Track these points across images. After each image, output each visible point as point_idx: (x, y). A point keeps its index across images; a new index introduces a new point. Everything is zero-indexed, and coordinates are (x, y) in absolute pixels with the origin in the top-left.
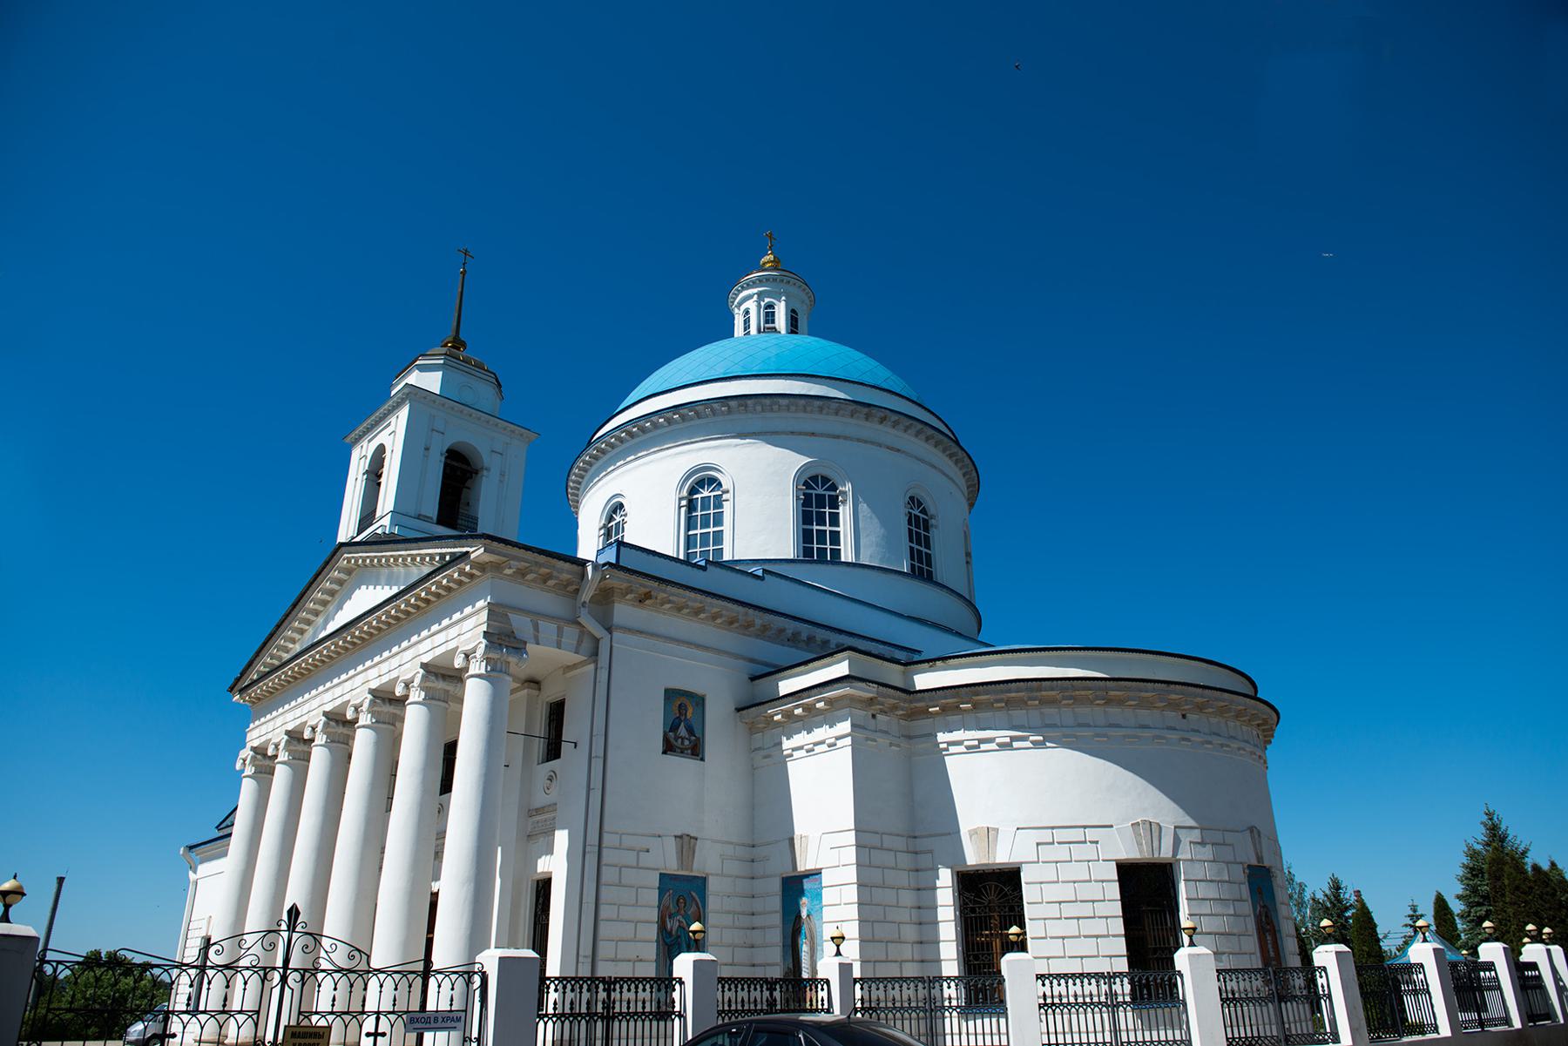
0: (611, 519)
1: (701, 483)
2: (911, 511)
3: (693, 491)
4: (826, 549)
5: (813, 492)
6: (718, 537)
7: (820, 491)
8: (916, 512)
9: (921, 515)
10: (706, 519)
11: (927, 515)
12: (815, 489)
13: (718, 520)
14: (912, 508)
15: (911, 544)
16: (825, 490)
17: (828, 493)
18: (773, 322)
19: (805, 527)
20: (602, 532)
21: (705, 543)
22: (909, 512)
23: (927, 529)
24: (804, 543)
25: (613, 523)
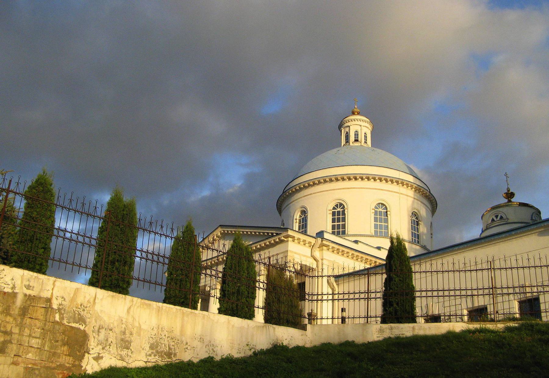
1: (337, 206)
2: (412, 218)
3: (334, 208)
5: (378, 210)
9: (416, 220)
11: (417, 219)
12: (379, 209)
13: (344, 220)
16: (382, 209)
17: (383, 211)
18: (358, 138)
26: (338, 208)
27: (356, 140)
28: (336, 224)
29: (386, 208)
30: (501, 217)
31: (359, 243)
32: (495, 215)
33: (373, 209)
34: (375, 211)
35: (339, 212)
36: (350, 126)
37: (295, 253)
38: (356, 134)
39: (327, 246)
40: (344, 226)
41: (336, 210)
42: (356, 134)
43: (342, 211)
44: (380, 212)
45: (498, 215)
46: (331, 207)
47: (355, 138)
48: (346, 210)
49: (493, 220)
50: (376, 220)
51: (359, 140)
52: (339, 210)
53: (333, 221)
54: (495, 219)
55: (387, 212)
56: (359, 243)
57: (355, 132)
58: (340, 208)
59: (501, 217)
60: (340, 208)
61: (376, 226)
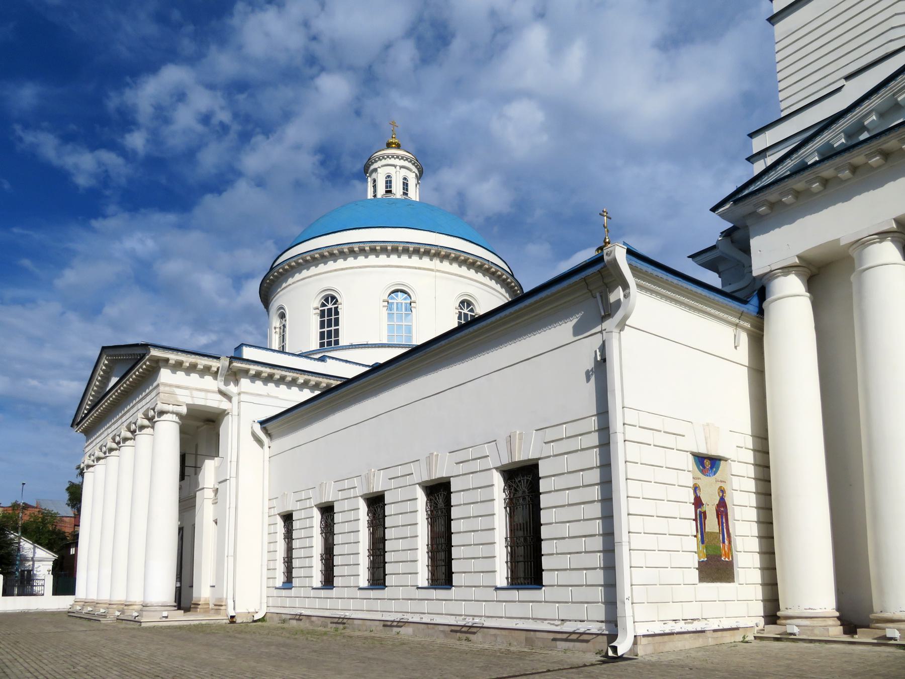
8: (466, 311)
9: (469, 313)
10: (330, 321)
13: (337, 323)
14: (461, 309)
17: (404, 302)
18: (391, 187)
22: (459, 312)
26: (328, 304)
27: (389, 192)
31: (328, 360)
33: (383, 301)
35: (330, 310)
36: (378, 169)
37: (178, 387)
38: (389, 183)
39: (246, 372)
41: (326, 308)
42: (389, 183)
43: (334, 308)
46: (317, 303)
47: (387, 187)
48: (340, 307)
52: (330, 306)
53: (322, 325)
56: (328, 360)
57: (386, 178)
58: (331, 303)
60: (331, 302)
61: (390, 328)
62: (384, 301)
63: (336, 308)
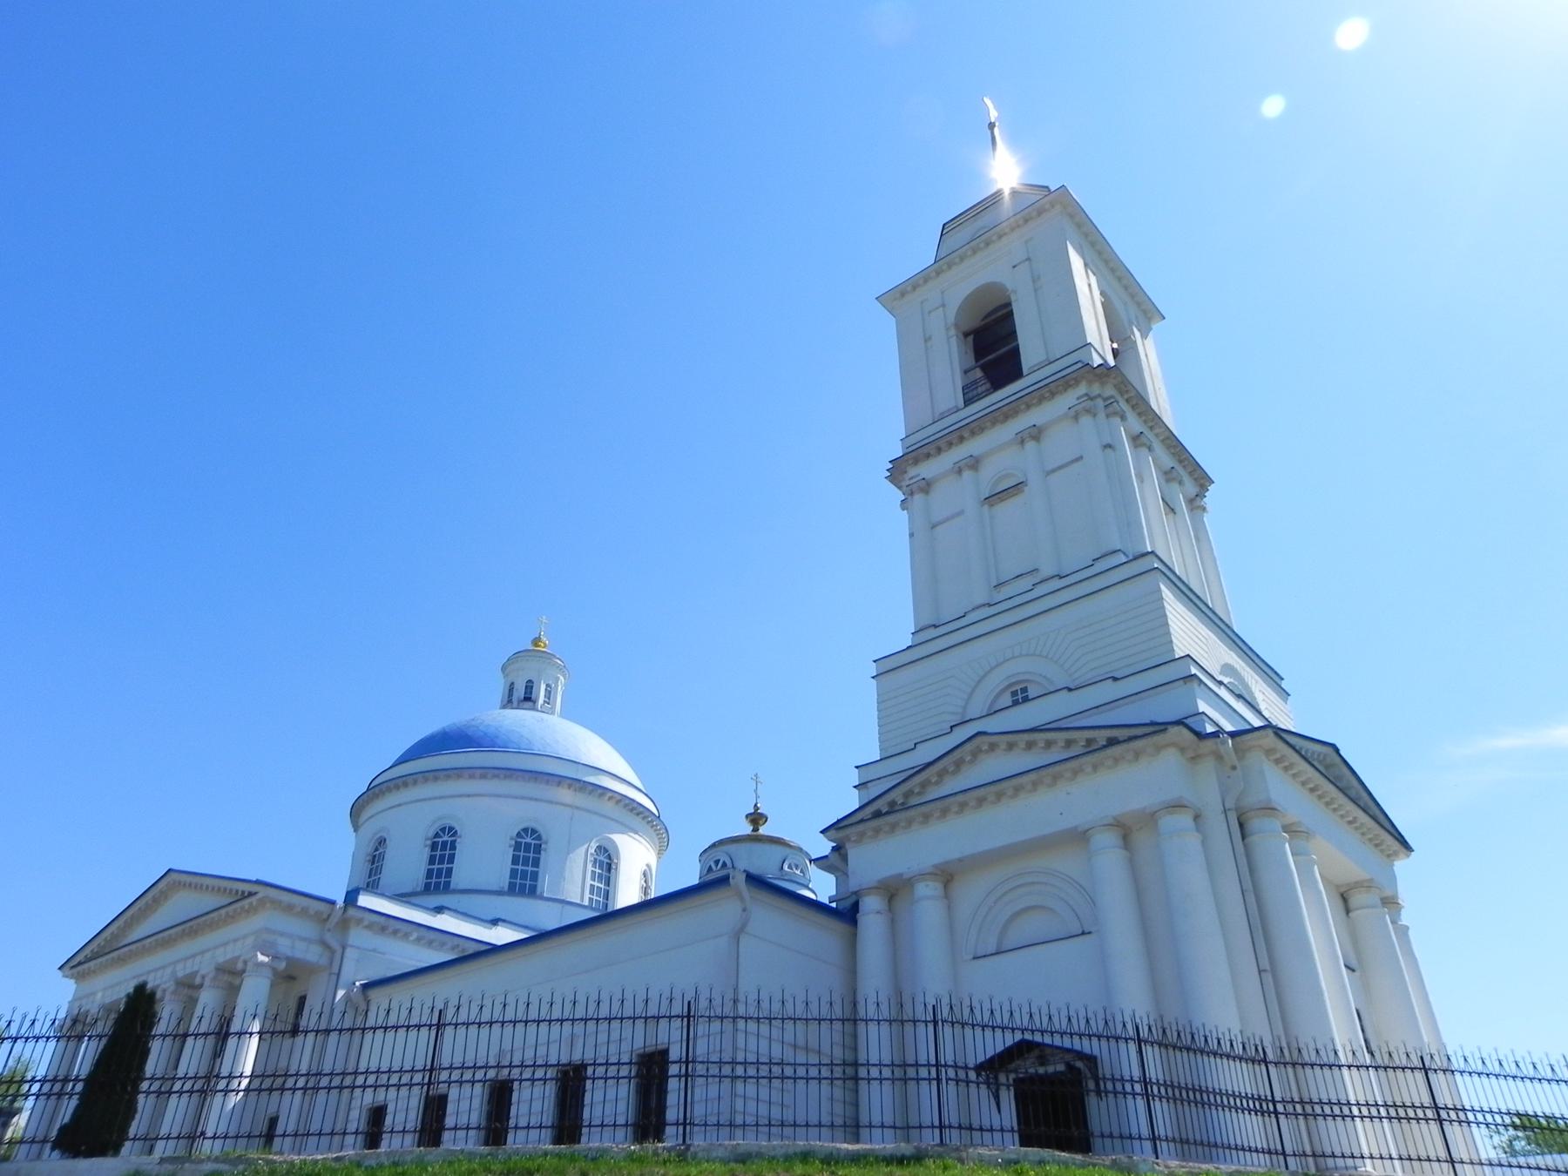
0: (376, 850)
1: (443, 830)
3: (437, 835)
4: (530, 885)
5: (524, 841)
6: (449, 872)
7: (528, 840)
8: (602, 858)
9: (606, 860)
13: (451, 859)
15: (593, 883)
17: (533, 842)
18: (531, 693)
19: (513, 867)
20: (368, 858)
21: (439, 875)
23: (609, 870)
24: (537, 872)
25: (378, 853)
28: (445, 866)
29: (539, 838)
30: (724, 865)
32: (715, 859)
34: (516, 842)
40: (449, 871)
41: (440, 840)
44: (528, 846)
45: (719, 860)
48: (458, 840)
49: (710, 869)
50: (515, 860)
51: (533, 696)
52: (445, 838)
54: (714, 867)
55: (541, 846)
58: (444, 834)
59: (724, 865)
60: (444, 834)
61: (513, 873)
62: (512, 839)
63: (453, 843)
